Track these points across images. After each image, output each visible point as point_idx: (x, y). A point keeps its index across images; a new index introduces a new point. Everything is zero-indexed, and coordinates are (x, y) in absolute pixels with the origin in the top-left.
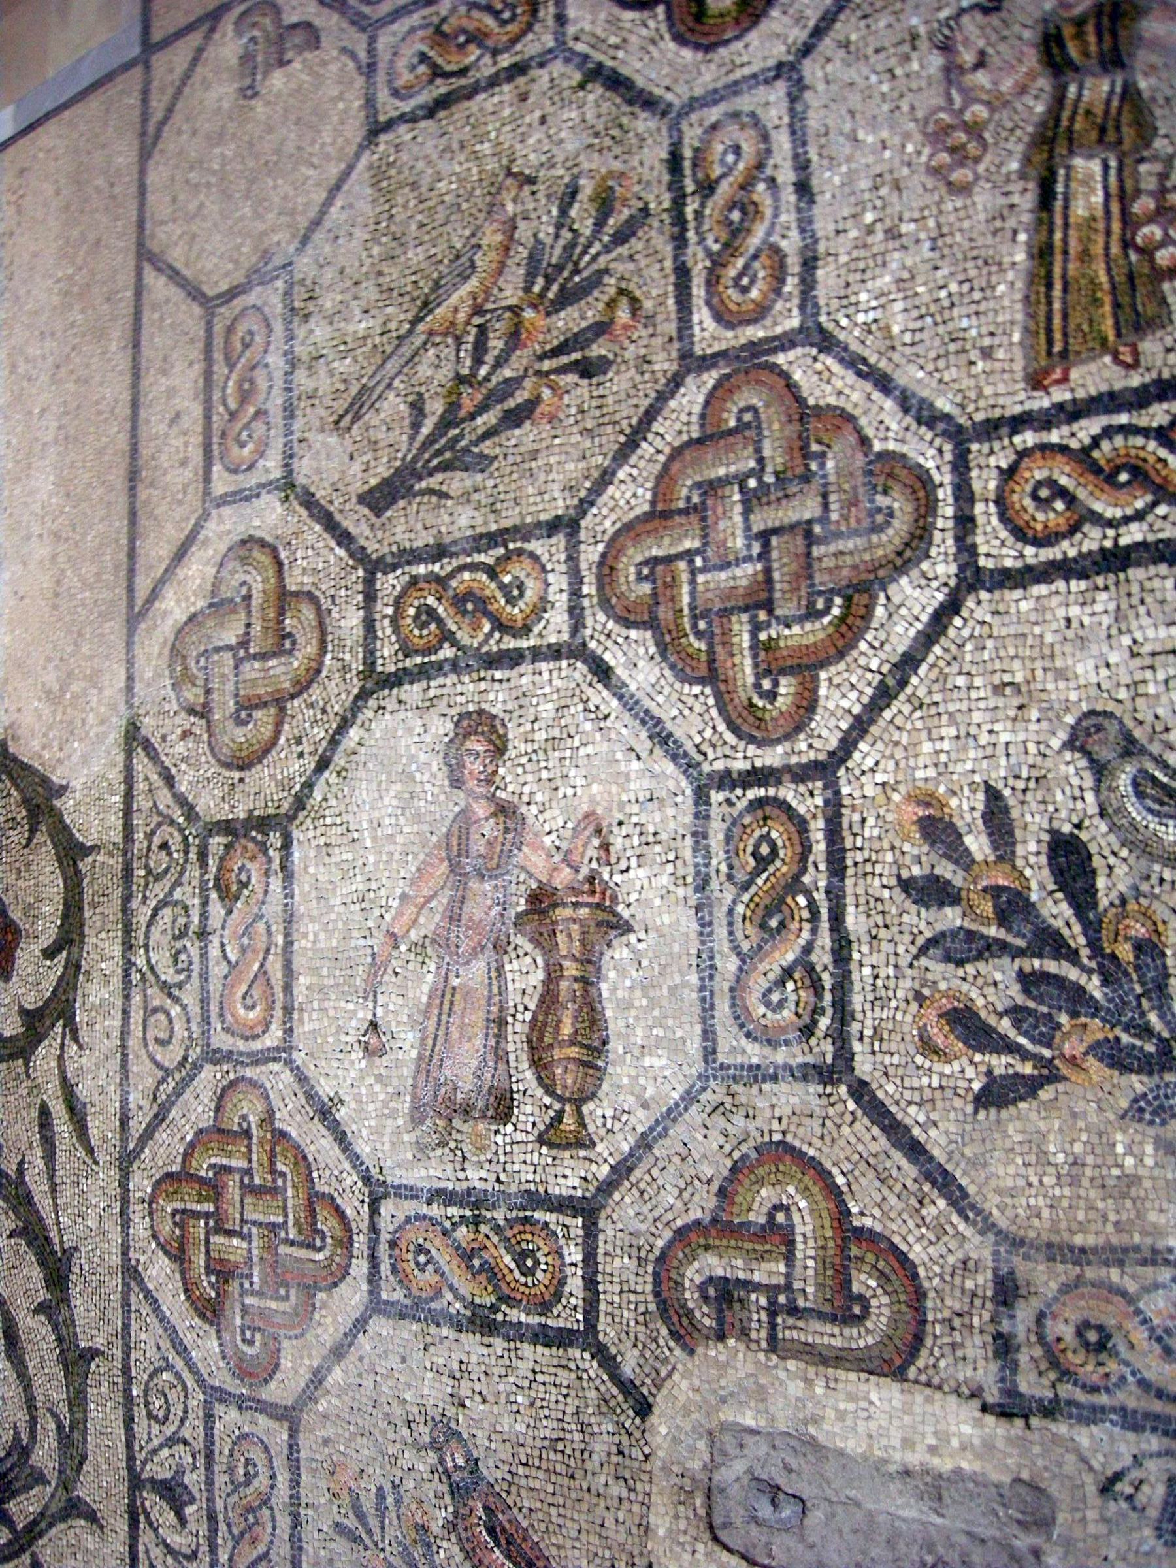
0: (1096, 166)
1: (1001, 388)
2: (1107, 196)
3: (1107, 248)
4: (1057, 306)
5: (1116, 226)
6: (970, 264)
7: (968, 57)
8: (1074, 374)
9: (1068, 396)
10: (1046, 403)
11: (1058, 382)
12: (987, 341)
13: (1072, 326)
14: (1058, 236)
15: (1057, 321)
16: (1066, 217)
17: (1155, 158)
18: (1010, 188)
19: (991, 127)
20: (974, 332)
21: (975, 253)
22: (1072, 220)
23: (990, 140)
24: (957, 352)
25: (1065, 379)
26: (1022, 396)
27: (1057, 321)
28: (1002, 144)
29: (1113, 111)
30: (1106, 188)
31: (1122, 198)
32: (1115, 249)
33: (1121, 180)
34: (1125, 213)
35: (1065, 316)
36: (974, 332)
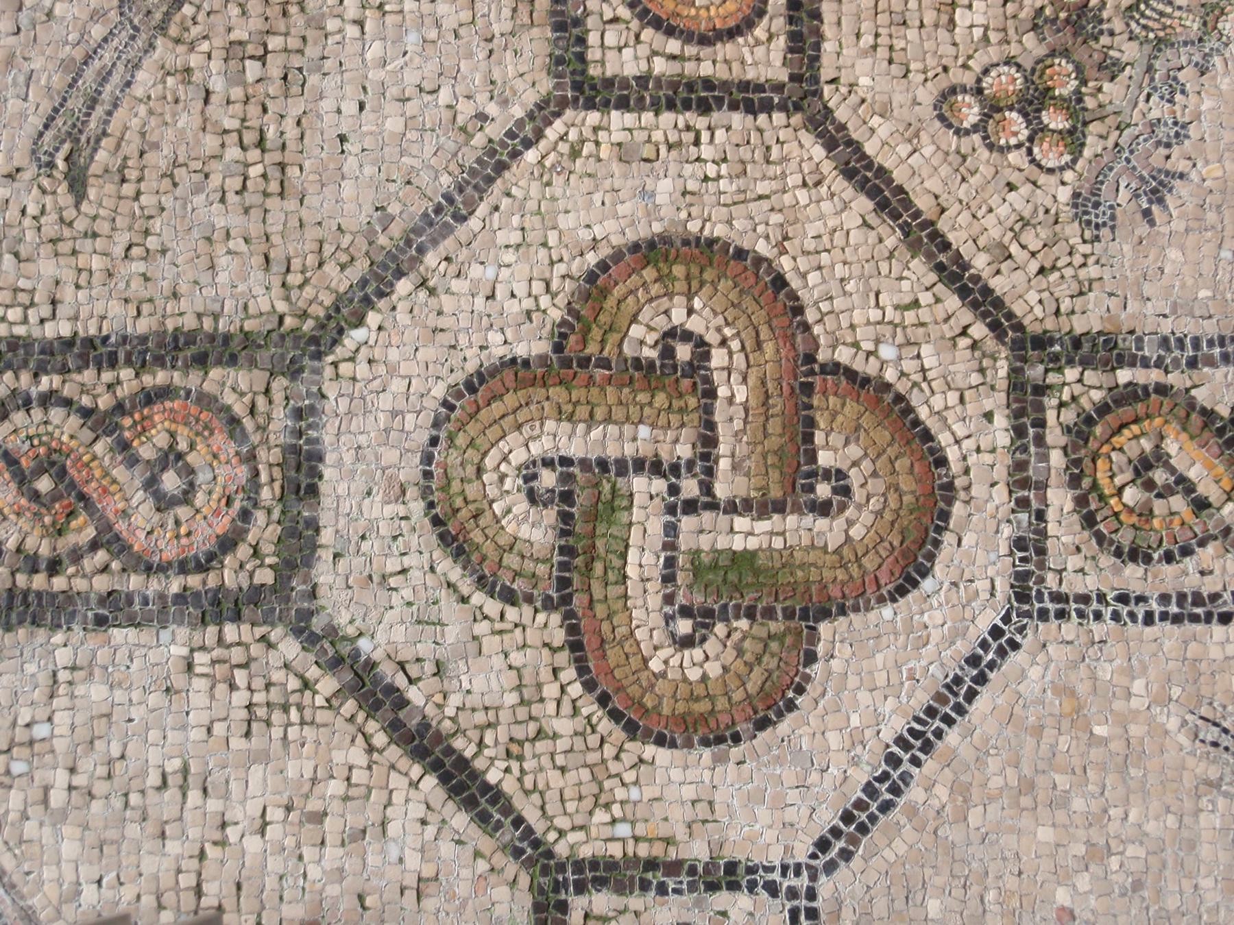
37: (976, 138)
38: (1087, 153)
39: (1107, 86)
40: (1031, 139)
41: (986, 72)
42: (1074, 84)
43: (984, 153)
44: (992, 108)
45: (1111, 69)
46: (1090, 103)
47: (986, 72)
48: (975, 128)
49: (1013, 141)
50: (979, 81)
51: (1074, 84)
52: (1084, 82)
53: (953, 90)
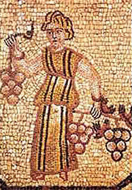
0: (59, 108)
1: (22, 177)
2: (62, 121)
3: (60, 139)
4: (42, 153)
5: (64, 132)
6: (14, 131)
7: (18, 54)
8: (46, 177)
9: (44, 184)
10: (37, 185)
11: (40, 179)
12: (18, 159)
13: (47, 160)
14: (45, 129)
15: (42, 158)
16: (48, 123)
17: (78, 112)
18: (30, 107)
19: (25, 82)
20: (13, 155)
21: (16, 127)
22: (50, 125)
23: (24, 87)
24: (7, 161)
25: (43, 178)
26: (28, 181)
27: (42, 158)
28: (28, 90)
29: (66, 91)
30: (62, 117)
31: (66, 122)
32: (63, 139)
33: (67, 116)
34: (67, 128)
35: (45, 158)
36: (13, 155)
37: (123, 152)
38: (126, 128)
39: (111, 123)
40: (123, 141)
41: (108, 150)
42: (110, 131)
43: (127, 151)
44: (117, 149)
45: (107, 122)
46: (115, 127)
47: (108, 150)
48: (121, 153)
49: (124, 144)
50: (110, 152)
51: (110, 131)
52: (110, 129)
53: (113, 158)
